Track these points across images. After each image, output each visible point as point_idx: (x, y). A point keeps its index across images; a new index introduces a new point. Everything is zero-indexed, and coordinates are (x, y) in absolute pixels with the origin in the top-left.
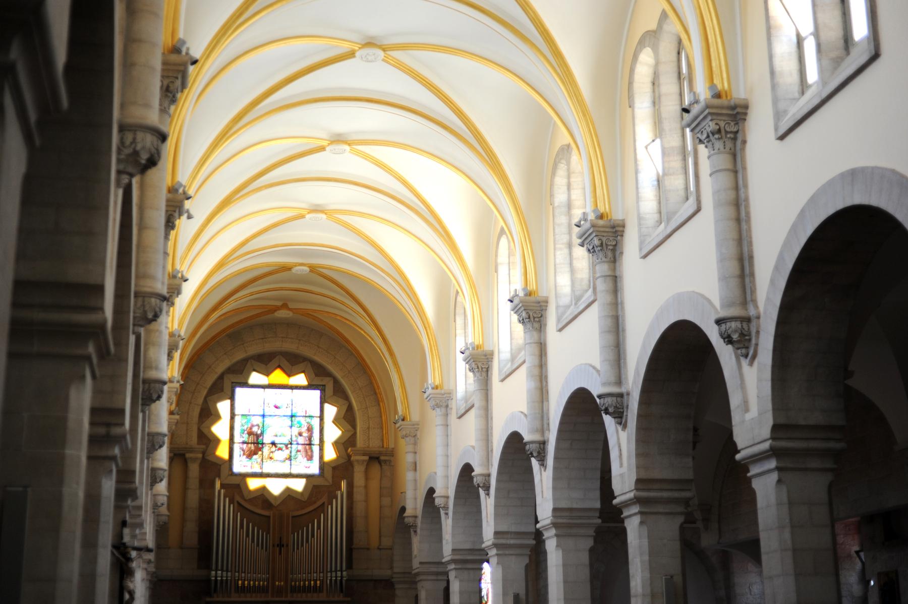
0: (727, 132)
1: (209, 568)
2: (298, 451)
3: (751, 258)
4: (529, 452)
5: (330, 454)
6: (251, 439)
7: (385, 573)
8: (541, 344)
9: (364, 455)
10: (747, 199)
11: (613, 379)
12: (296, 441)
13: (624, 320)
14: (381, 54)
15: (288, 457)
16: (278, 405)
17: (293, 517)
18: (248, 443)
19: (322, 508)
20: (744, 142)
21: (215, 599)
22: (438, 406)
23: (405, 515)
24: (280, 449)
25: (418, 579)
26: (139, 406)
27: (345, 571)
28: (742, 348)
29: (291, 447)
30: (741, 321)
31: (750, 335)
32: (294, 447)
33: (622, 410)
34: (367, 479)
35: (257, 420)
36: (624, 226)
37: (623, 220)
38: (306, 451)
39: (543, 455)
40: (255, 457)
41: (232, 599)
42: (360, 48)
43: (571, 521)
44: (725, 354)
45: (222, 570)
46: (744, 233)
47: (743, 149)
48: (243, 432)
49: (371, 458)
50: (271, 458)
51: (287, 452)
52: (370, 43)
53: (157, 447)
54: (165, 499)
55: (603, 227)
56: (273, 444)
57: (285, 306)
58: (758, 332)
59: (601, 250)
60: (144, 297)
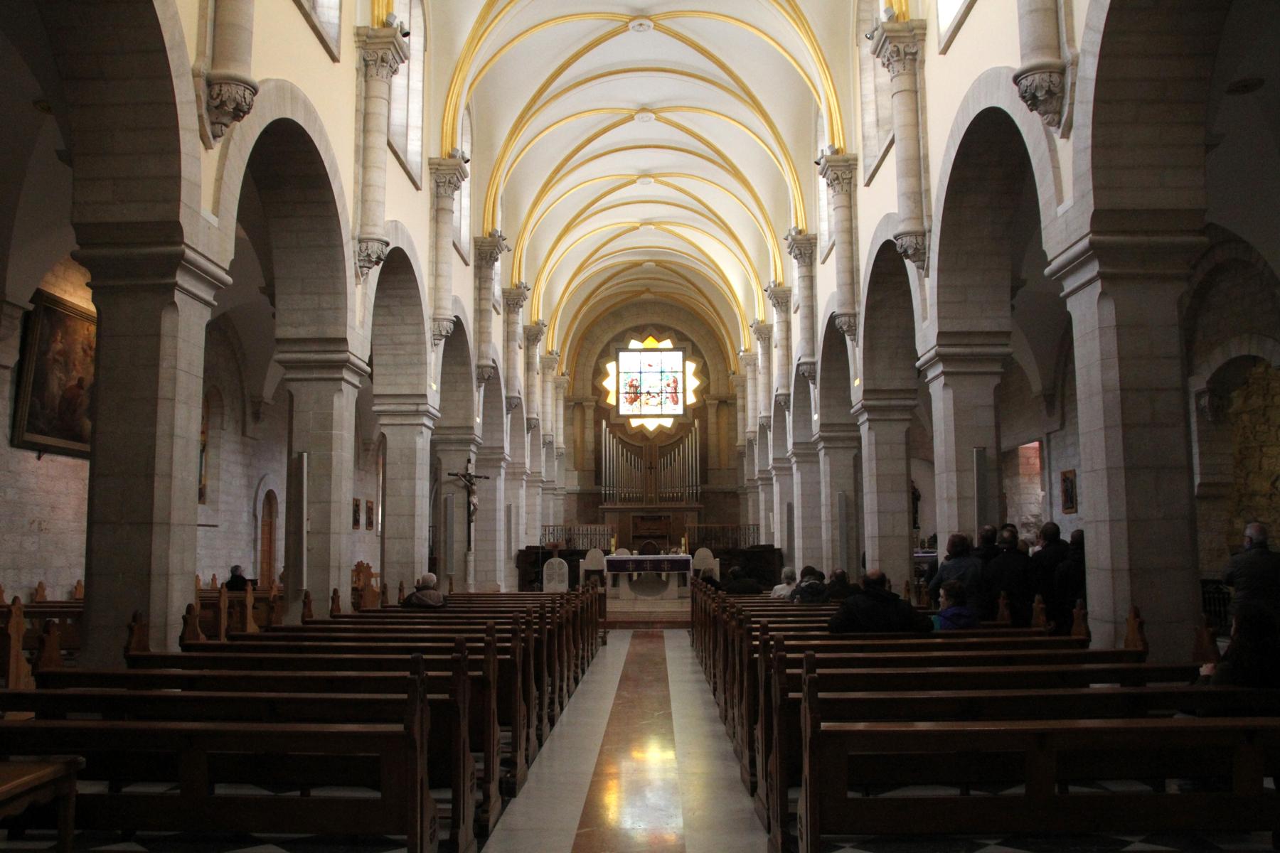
0: (844, 179)
1: (601, 484)
5: (691, 399)
6: (632, 390)
7: (729, 486)
9: (716, 399)
10: (857, 228)
11: (808, 352)
14: (654, 116)
19: (681, 440)
20: (856, 185)
21: (605, 506)
22: (748, 364)
24: (654, 397)
25: (748, 491)
26: (472, 383)
32: (664, 395)
34: (718, 417)
36: (816, 239)
38: (673, 398)
43: (806, 452)
47: (855, 191)
49: (720, 402)
52: (644, 109)
55: (800, 240)
56: (648, 393)
57: (648, 290)
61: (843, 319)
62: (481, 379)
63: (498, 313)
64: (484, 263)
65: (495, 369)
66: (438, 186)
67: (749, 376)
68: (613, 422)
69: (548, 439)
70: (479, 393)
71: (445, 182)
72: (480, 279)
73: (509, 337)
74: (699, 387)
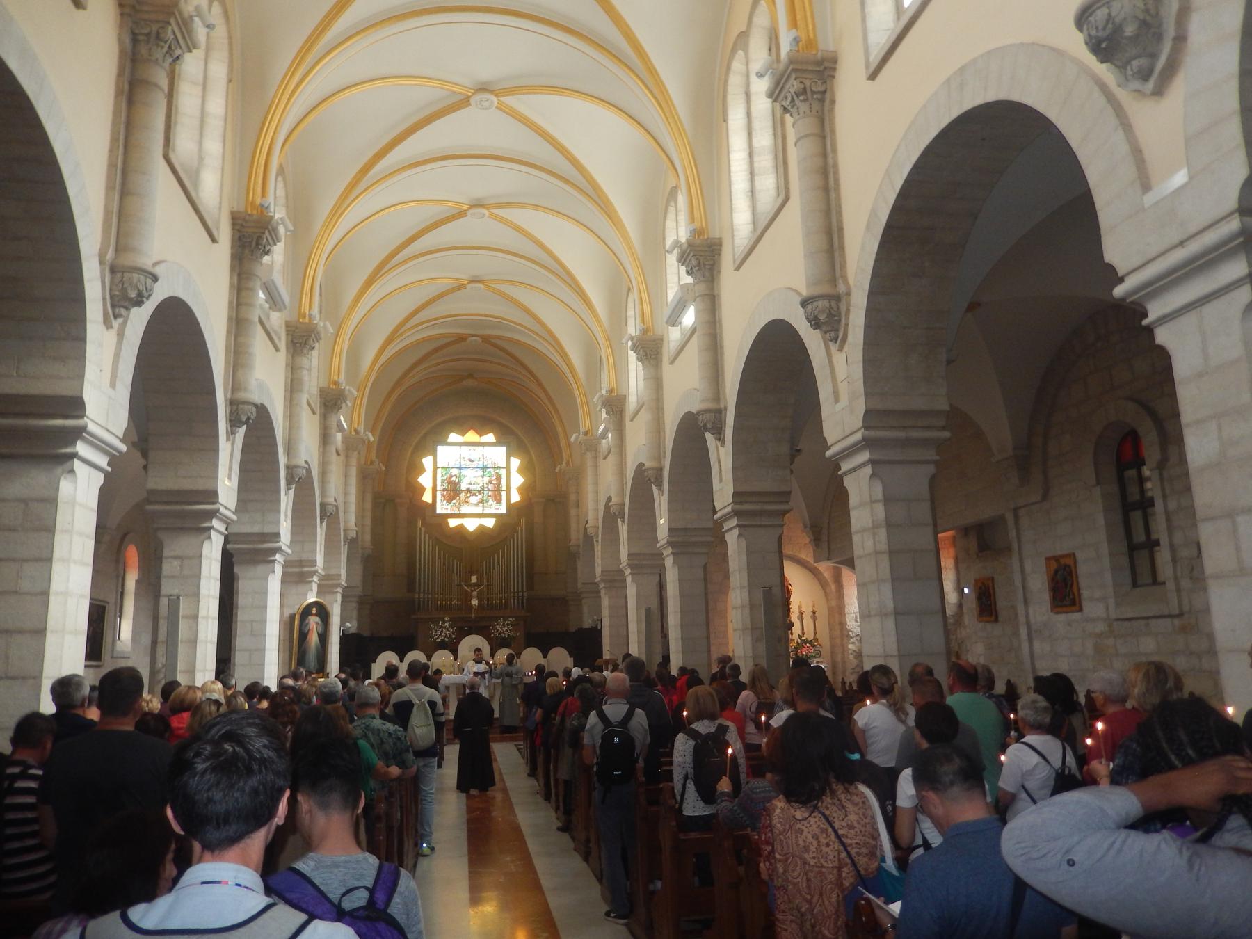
0: (813, 93)
2: (490, 496)
3: (841, 229)
4: (647, 479)
5: (516, 498)
8: (657, 379)
10: (835, 166)
12: (488, 487)
13: (721, 338)
15: (481, 501)
16: (472, 459)
18: (447, 490)
20: (833, 102)
22: (587, 450)
23: (571, 544)
24: (475, 495)
28: (831, 331)
29: (483, 493)
30: (829, 300)
31: (839, 315)
32: (485, 492)
33: (720, 426)
35: (455, 472)
37: (720, 239)
38: (495, 496)
39: (660, 480)
40: (454, 501)
42: (473, 94)
44: (812, 340)
45: (424, 593)
46: (833, 203)
47: (832, 110)
48: (443, 481)
50: (467, 502)
51: (480, 496)
54: (355, 533)
56: (468, 490)
57: (471, 376)
58: (848, 311)
59: (699, 269)
60: (123, 272)
61: (820, 304)
62: (234, 422)
63: (277, 349)
64: (247, 251)
65: (262, 411)
66: (135, 40)
67: (589, 463)
69: (353, 534)
70: (233, 445)
71: (148, 35)
72: (239, 275)
73: (293, 387)
74: (523, 484)
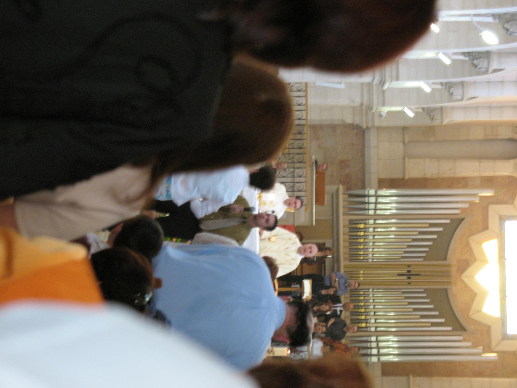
17: (446, 290)
21: (341, 197)
27: (379, 359)
41: (341, 217)
45: (376, 203)
53: (506, 26)
54: (460, 97)
68: (494, 210)
